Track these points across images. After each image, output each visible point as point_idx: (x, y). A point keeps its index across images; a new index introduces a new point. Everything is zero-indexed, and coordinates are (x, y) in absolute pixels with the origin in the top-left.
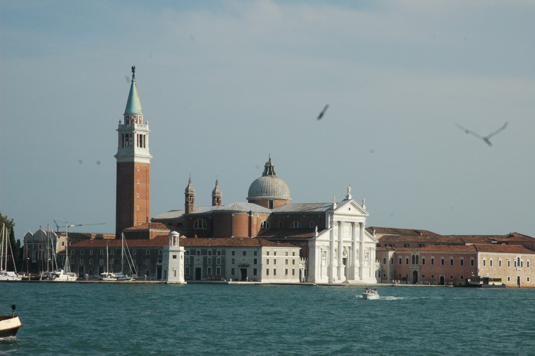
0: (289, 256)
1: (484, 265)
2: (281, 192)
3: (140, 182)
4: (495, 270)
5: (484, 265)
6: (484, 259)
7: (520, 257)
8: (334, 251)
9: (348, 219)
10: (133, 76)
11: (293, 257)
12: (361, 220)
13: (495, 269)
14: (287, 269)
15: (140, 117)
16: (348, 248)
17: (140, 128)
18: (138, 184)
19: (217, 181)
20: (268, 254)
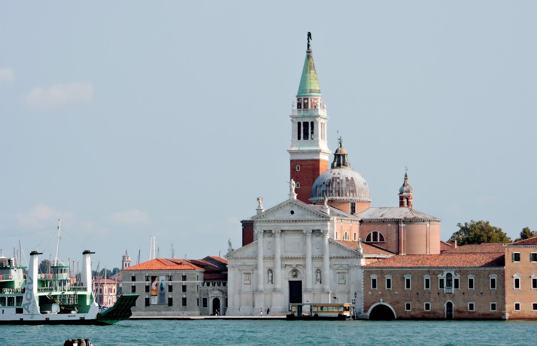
0: (175, 280)
1: (374, 286)
2: (323, 191)
3: (301, 186)
4: (396, 294)
5: (374, 286)
6: (374, 277)
7: (453, 273)
8: (262, 271)
9: (286, 227)
10: (309, 46)
11: (184, 282)
12: (319, 225)
13: (396, 293)
14: (172, 299)
15: (305, 99)
16: (301, 267)
17: (302, 115)
18: (299, 188)
19: (406, 176)
20: (134, 279)
